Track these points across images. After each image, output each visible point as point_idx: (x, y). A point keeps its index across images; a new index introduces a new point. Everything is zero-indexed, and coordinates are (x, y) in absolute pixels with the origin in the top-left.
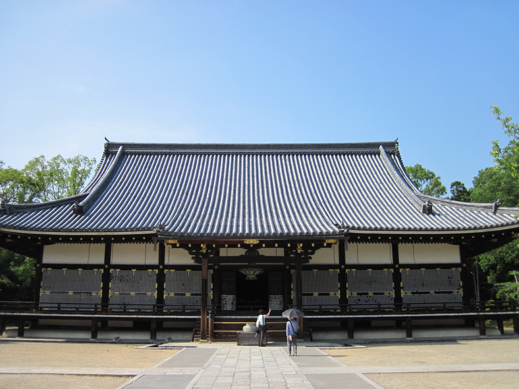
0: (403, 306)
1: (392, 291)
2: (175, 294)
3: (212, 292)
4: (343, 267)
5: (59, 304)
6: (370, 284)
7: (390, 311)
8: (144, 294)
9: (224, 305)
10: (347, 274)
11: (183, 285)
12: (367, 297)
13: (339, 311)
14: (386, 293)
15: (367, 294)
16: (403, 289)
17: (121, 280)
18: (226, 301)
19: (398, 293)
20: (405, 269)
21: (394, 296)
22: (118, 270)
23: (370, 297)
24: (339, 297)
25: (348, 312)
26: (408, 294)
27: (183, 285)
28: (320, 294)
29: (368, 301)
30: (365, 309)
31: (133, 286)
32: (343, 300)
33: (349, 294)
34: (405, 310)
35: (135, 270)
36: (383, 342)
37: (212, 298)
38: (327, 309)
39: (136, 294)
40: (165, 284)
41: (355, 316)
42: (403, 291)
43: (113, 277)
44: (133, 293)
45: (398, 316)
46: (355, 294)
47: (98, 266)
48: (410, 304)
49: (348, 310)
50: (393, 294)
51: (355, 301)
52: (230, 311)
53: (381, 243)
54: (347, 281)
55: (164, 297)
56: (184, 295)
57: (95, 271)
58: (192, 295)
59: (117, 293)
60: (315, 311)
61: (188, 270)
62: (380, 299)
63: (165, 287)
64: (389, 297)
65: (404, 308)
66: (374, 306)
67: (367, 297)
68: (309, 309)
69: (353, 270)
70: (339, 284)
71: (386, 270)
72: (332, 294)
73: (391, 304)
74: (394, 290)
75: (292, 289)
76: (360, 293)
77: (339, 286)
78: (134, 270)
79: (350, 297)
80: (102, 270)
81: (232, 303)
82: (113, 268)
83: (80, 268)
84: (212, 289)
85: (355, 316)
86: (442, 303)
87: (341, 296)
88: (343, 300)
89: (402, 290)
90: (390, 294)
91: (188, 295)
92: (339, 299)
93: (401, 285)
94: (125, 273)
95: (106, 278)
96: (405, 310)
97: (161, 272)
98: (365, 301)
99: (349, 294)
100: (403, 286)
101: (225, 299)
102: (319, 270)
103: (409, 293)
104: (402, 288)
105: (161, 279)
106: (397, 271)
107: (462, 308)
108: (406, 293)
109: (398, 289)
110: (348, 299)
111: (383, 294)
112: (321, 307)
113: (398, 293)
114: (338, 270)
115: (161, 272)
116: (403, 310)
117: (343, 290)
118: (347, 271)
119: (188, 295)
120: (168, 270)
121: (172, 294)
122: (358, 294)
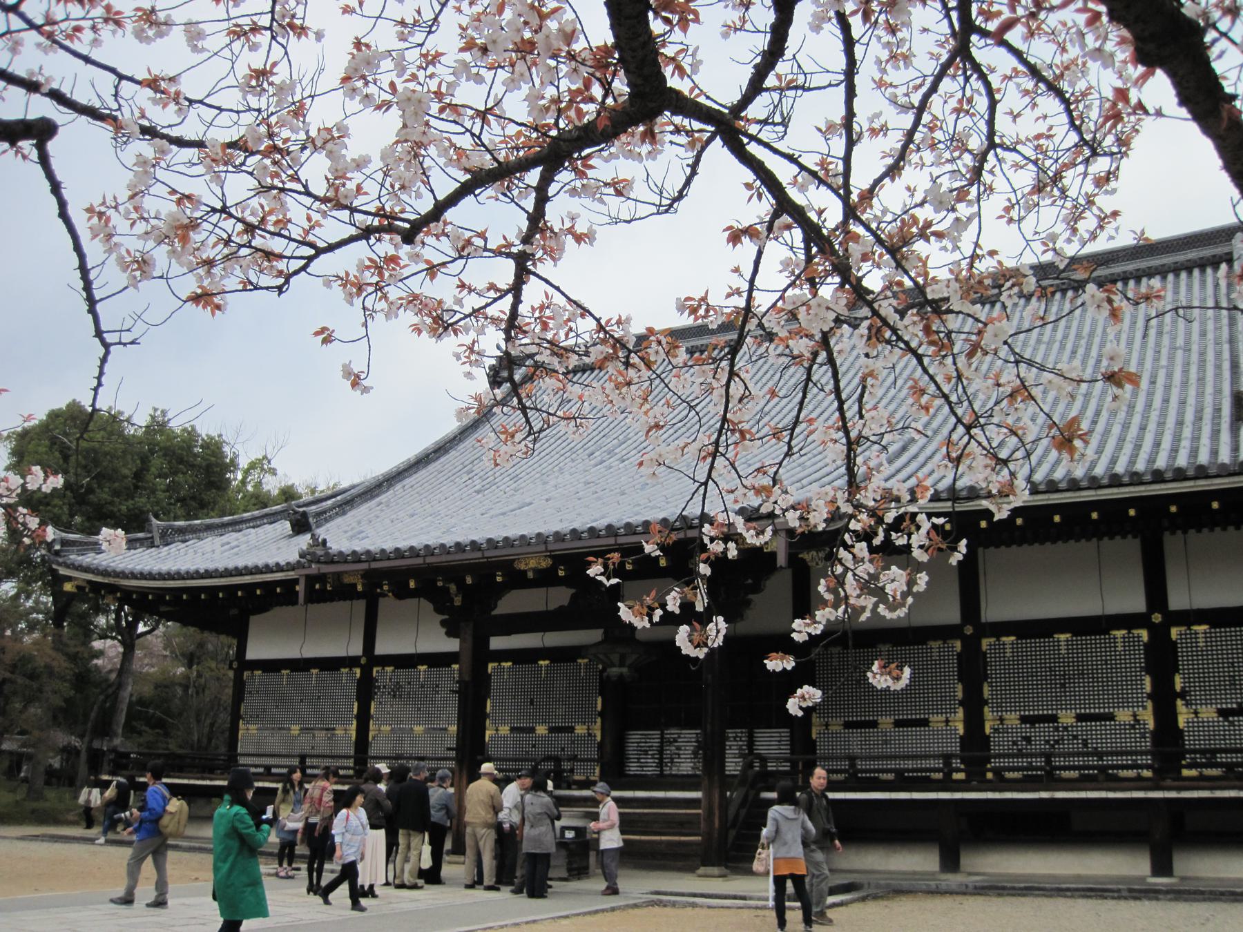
0: (1185, 759)
1: (1144, 707)
2: (513, 729)
3: (599, 720)
4: (1157, 618)
5: (303, 758)
6: (1063, 686)
7: (1202, 778)
8: (441, 729)
9: (672, 759)
10: (985, 653)
11: (532, 703)
12: (1057, 729)
13: (960, 776)
14: (1124, 716)
15: (1053, 719)
16: (1183, 698)
17: (394, 696)
18: (678, 748)
19: (1165, 715)
20: (1189, 625)
21: (1151, 725)
22: (389, 669)
23: (1066, 729)
24: (961, 732)
25: (990, 781)
26: (833, 728)
27: (532, 703)
28: (898, 724)
29: (1057, 742)
30: (1103, 769)
31: (419, 709)
32: (975, 740)
33: (994, 720)
34: (1193, 773)
35: (425, 667)
36: (1026, 888)
37: (599, 738)
38: (921, 770)
39: (427, 731)
40: (489, 702)
41: (958, 795)
42: (1187, 705)
43: (379, 687)
44: (419, 729)
45: (1111, 795)
46: (1012, 719)
47: (1128, 621)
48: (1214, 752)
49: (990, 775)
50: (1148, 717)
51: (1015, 743)
52: (688, 776)
53: (1130, 536)
54: (986, 677)
55: (487, 739)
56: (532, 730)
57: (1196, 633)
58: (551, 730)
59: (387, 728)
60: (884, 776)
61: (541, 662)
62: (1099, 736)
63: (488, 709)
64: (1133, 727)
65: (1189, 767)
66: (1078, 761)
67: (1057, 729)
68: (908, 771)
69: (1004, 639)
70: (960, 687)
71: (1119, 633)
72: (937, 719)
73: (1142, 753)
74: (1149, 704)
75: (986, 703)
76: (1029, 716)
77: (960, 695)
78: (422, 668)
79: (996, 730)
80: (958, 645)
81: (695, 753)
82: (493, 661)
83: (1118, 629)
84: (961, 703)
85: (958, 795)
86: (1041, 755)
87: (966, 728)
88: (975, 740)
89: (1179, 702)
90: (1135, 715)
91: (541, 730)
92: (961, 737)
93: (1178, 687)
94: (403, 675)
95: (366, 691)
96: (1193, 773)
97: (971, 646)
98: (1047, 742)
99: (994, 720)
100: (1183, 688)
101: (675, 741)
102: (1075, 634)
103: (1208, 713)
104: (1183, 695)
105: (366, 691)
106: (1159, 634)
107: (1155, 771)
108: (1196, 713)
109: (1164, 700)
110: (989, 737)
111: (1111, 717)
112: (853, 765)
113: (1165, 715)
114: (1144, 634)
115: (971, 646)
116: (1185, 772)
117: (974, 707)
118: (1175, 632)
119: (541, 730)
120: (496, 664)
121: (504, 730)
122: (1024, 719)
